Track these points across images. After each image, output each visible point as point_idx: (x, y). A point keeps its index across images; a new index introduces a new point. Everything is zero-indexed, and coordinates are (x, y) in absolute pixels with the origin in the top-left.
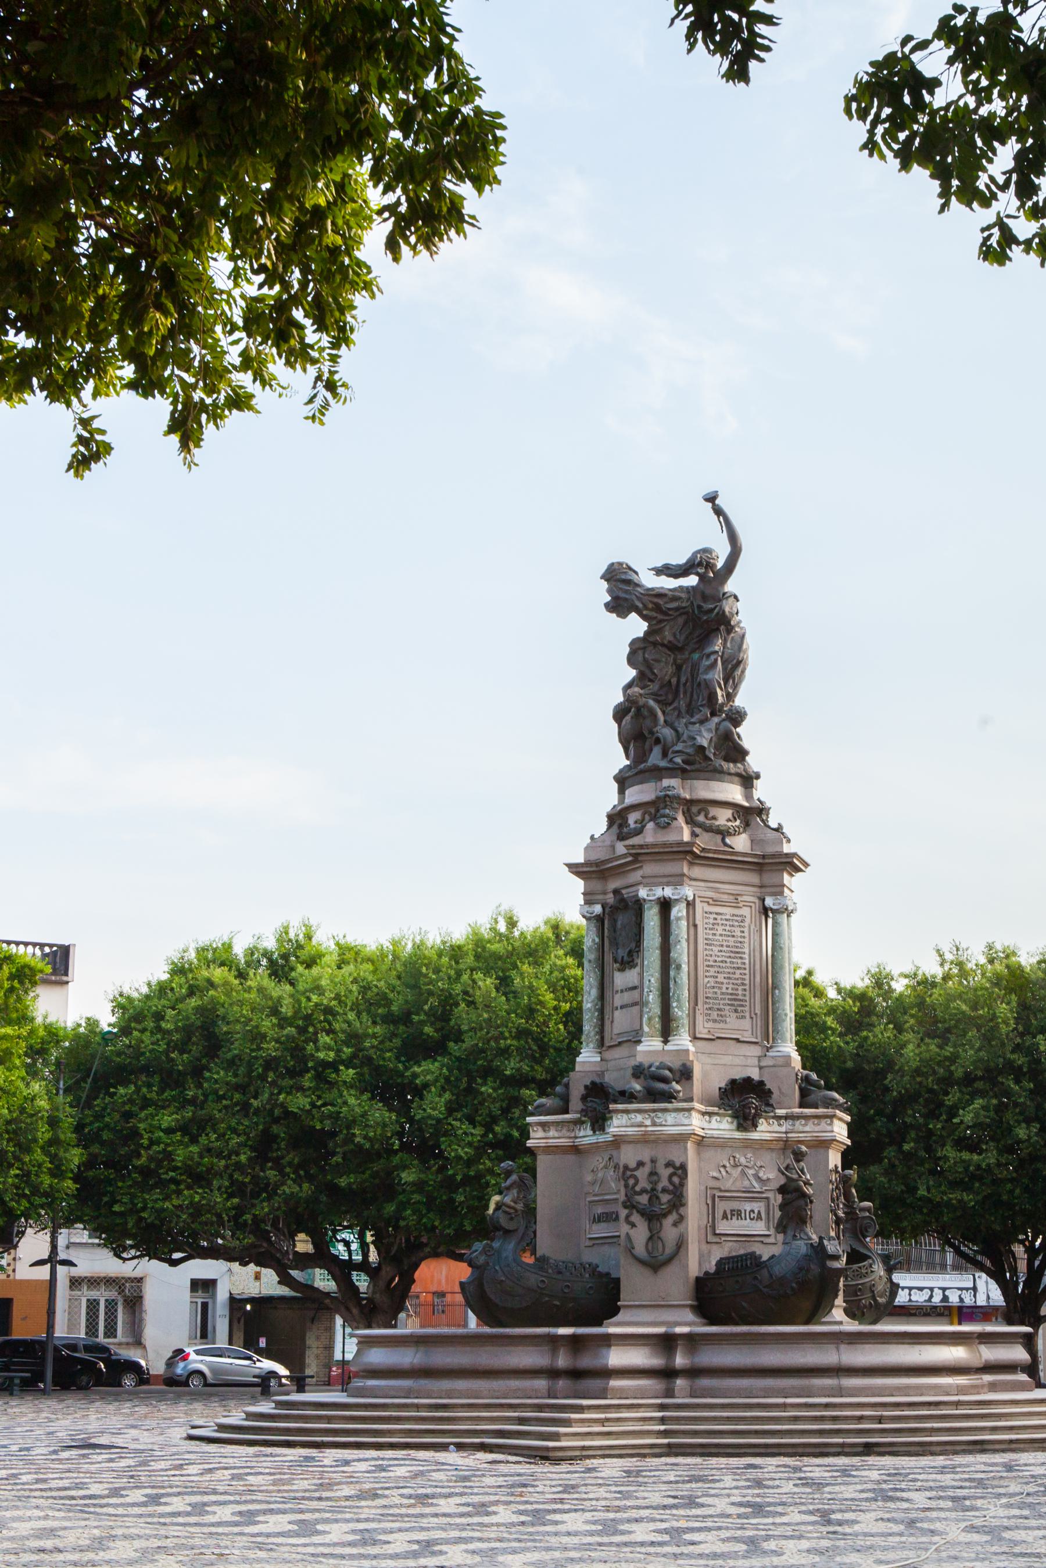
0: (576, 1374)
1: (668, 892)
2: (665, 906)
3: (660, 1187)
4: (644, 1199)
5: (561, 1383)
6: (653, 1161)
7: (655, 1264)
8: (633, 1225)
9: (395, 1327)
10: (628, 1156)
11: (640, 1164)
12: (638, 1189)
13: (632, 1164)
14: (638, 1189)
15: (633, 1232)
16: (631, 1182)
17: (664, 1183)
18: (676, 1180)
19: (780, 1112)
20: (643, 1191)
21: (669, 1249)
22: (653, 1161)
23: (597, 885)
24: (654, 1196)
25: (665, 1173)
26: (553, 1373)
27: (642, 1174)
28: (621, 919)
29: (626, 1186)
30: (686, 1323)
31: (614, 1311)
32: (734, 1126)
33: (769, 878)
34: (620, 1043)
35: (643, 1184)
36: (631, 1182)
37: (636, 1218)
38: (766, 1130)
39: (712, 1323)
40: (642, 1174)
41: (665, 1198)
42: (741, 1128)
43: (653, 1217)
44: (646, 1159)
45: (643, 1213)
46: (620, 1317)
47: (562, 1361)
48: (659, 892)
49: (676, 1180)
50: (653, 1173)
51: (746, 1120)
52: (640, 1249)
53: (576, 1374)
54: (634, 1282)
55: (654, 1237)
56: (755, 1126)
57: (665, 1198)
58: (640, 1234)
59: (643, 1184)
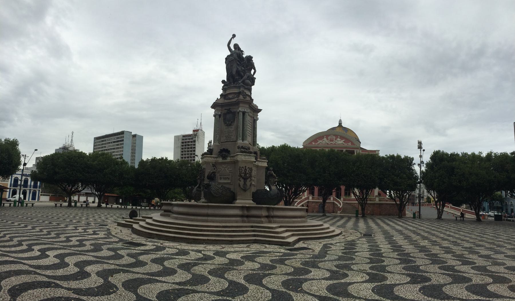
0: (247, 216)
2: (244, 113)
4: (243, 175)
5: (245, 219)
6: (245, 167)
7: (245, 190)
9: (234, 204)
11: (243, 167)
17: (247, 172)
21: (248, 188)
22: (245, 167)
23: (219, 108)
24: (245, 174)
25: (248, 170)
26: (242, 216)
28: (228, 116)
31: (236, 199)
33: (255, 114)
35: (243, 171)
43: (245, 179)
45: (243, 178)
46: (238, 201)
47: (246, 213)
52: (242, 186)
53: (247, 216)
55: (245, 184)
57: (248, 175)
58: (242, 183)
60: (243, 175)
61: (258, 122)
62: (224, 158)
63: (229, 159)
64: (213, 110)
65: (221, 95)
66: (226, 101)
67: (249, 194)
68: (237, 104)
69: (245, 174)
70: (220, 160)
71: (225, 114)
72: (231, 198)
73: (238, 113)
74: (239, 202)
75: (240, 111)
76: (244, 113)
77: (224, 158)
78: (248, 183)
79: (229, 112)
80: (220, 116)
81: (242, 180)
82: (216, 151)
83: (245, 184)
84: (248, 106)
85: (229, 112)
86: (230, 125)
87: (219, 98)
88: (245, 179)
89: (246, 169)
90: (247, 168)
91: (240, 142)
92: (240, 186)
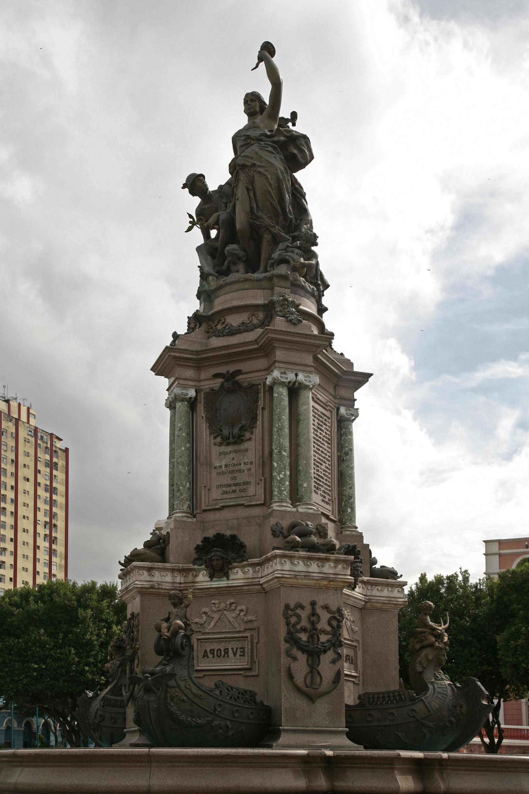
1: (301, 377)
2: (295, 391)
3: (319, 626)
6: (313, 604)
8: (295, 659)
12: (298, 627)
13: (292, 606)
14: (298, 627)
15: (294, 666)
16: (293, 620)
19: (366, 579)
20: (304, 630)
22: (313, 604)
25: (325, 616)
27: (304, 614)
29: (288, 624)
34: (223, 508)
35: (304, 623)
36: (293, 620)
39: (366, 748)
41: (323, 638)
43: (314, 654)
44: (306, 604)
45: (303, 649)
46: (283, 739)
48: (291, 377)
52: (299, 680)
57: (323, 638)
59: (304, 623)
60: (304, 637)
61: (355, 425)
62: (219, 570)
63: (238, 576)
64: (164, 382)
65: (196, 320)
66: (216, 342)
68: (265, 350)
69: (313, 631)
70: (203, 579)
71: (212, 397)
72: (264, 727)
73: (271, 389)
75: (275, 382)
77: (219, 570)
78: (326, 668)
79: (231, 384)
80: (192, 404)
81: (302, 658)
82: (182, 546)
84: (309, 359)
85: (231, 384)
86: (239, 439)
87: (182, 329)
88: (314, 654)
89: (314, 613)
90: (319, 611)
91: (282, 506)
92: (290, 676)
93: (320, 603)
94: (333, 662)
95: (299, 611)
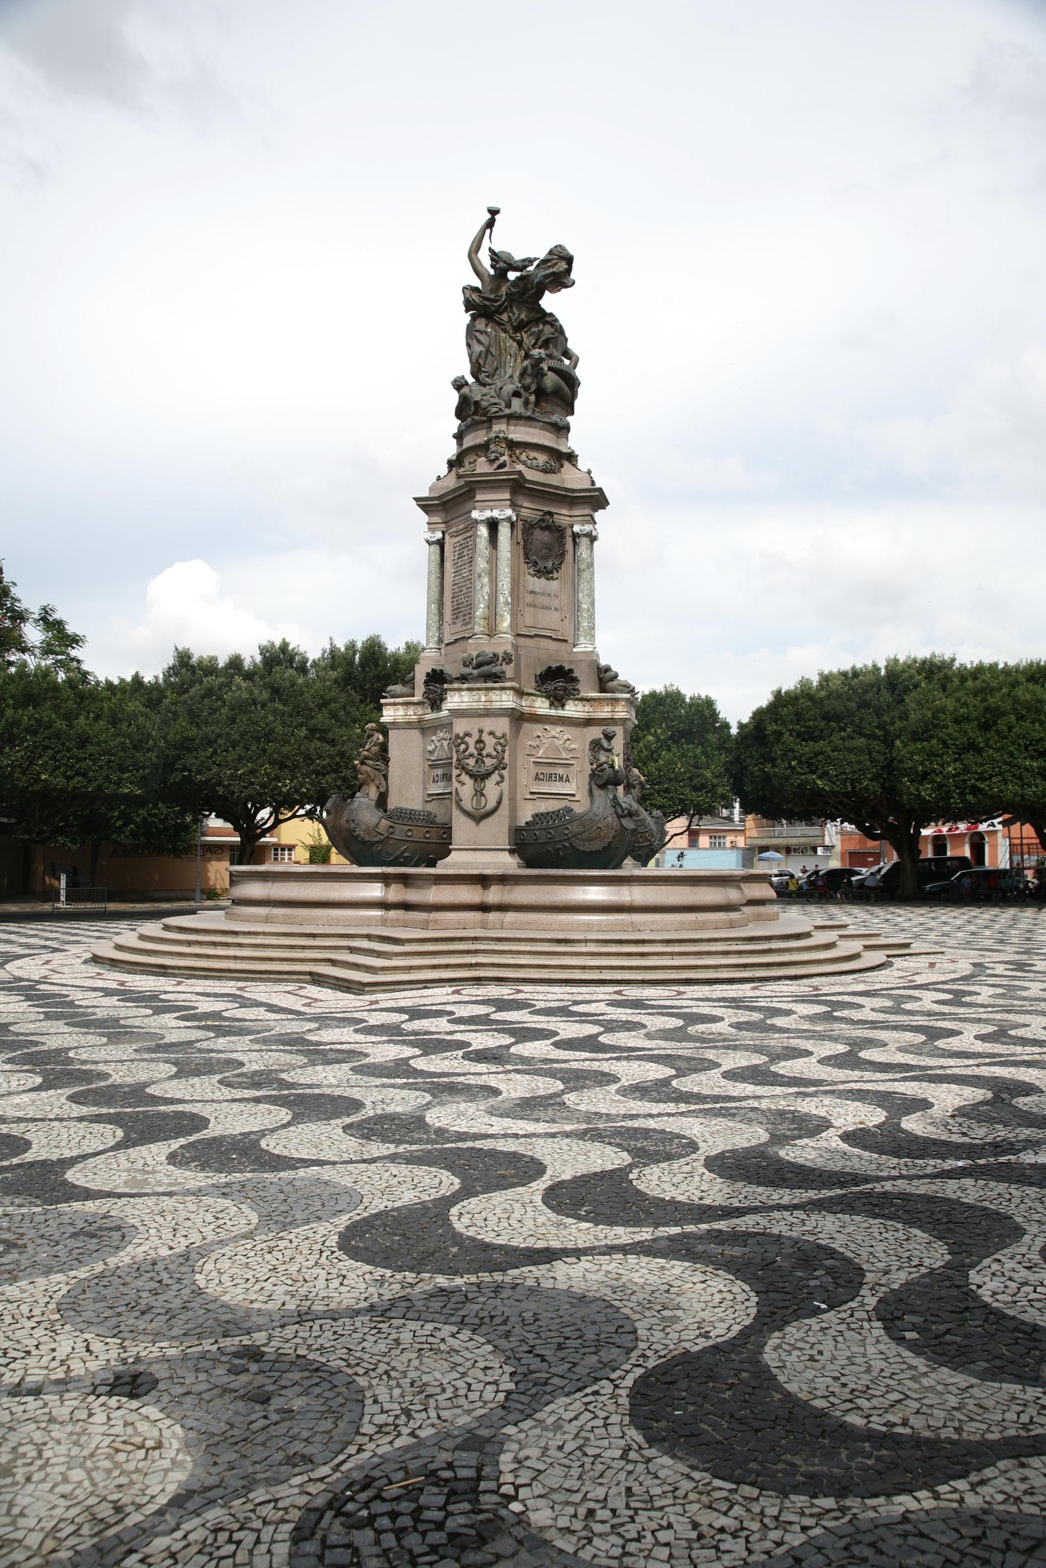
1: (496, 514)
3: (484, 753)
4: (471, 762)
7: (479, 817)
10: (460, 727)
16: (463, 747)
17: (489, 749)
18: (499, 748)
21: (491, 804)
27: (471, 741)
30: (507, 863)
31: (448, 852)
32: (547, 703)
35: (472, 750)
37: (465, 778)
38: (573, 709)
40: (471, 741)
41: (489, 762)
42: (552, 705)
45: (471, 776)
46: (454, 857)
48: (488, 514)
49: (499, 748)
50: (480, 741)
51: (558, 700)
54: (462, 829)
55: (479, 793)
56: (563, 706)
57: (489, 762)
67: (497, 829)
74: (455, 862)
76: (493, 525)
83: (479, 793)
89: (480, 741)
90: (485, 737)
93: (487, 730)
94: (498, 783)
95: (467, 739)
